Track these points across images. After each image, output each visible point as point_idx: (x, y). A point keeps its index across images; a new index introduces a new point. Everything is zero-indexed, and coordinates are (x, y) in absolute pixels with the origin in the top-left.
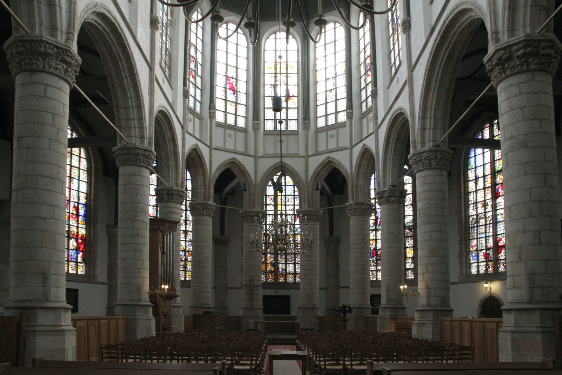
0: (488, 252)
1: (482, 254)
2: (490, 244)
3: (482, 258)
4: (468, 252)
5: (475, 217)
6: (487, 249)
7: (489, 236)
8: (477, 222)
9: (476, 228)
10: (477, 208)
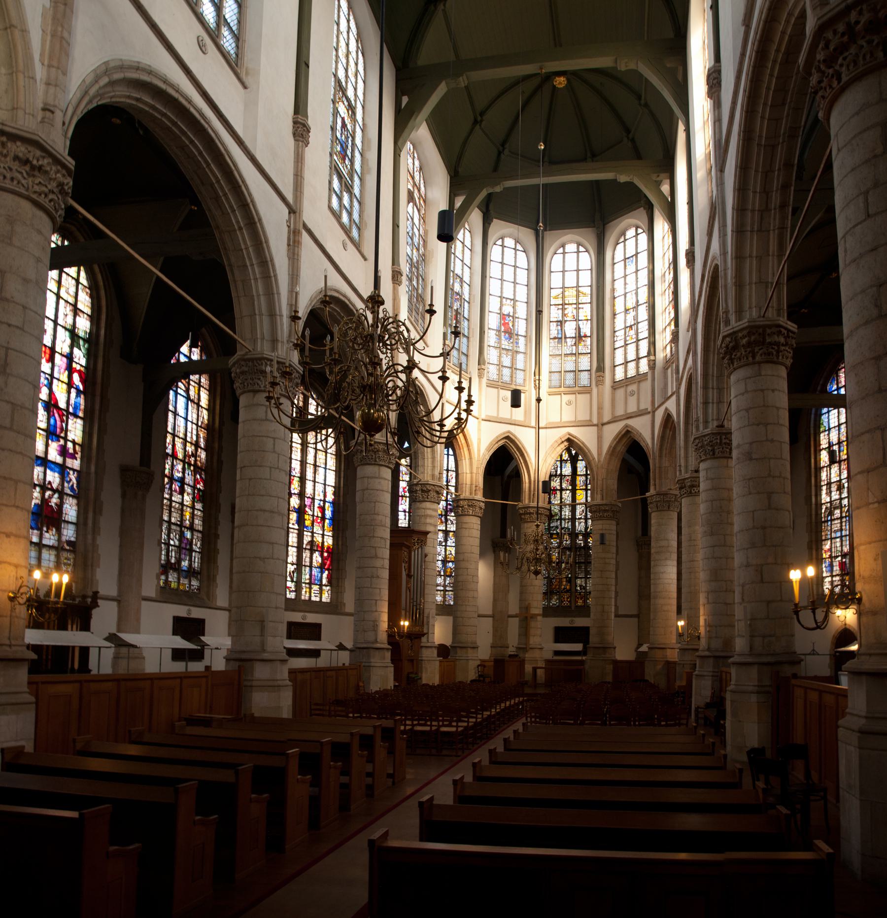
0: (844, 560)
5: (829, 505)
7: (846, 536)
8: (831, 513)
9: (829, 523)
10: (831, 492)
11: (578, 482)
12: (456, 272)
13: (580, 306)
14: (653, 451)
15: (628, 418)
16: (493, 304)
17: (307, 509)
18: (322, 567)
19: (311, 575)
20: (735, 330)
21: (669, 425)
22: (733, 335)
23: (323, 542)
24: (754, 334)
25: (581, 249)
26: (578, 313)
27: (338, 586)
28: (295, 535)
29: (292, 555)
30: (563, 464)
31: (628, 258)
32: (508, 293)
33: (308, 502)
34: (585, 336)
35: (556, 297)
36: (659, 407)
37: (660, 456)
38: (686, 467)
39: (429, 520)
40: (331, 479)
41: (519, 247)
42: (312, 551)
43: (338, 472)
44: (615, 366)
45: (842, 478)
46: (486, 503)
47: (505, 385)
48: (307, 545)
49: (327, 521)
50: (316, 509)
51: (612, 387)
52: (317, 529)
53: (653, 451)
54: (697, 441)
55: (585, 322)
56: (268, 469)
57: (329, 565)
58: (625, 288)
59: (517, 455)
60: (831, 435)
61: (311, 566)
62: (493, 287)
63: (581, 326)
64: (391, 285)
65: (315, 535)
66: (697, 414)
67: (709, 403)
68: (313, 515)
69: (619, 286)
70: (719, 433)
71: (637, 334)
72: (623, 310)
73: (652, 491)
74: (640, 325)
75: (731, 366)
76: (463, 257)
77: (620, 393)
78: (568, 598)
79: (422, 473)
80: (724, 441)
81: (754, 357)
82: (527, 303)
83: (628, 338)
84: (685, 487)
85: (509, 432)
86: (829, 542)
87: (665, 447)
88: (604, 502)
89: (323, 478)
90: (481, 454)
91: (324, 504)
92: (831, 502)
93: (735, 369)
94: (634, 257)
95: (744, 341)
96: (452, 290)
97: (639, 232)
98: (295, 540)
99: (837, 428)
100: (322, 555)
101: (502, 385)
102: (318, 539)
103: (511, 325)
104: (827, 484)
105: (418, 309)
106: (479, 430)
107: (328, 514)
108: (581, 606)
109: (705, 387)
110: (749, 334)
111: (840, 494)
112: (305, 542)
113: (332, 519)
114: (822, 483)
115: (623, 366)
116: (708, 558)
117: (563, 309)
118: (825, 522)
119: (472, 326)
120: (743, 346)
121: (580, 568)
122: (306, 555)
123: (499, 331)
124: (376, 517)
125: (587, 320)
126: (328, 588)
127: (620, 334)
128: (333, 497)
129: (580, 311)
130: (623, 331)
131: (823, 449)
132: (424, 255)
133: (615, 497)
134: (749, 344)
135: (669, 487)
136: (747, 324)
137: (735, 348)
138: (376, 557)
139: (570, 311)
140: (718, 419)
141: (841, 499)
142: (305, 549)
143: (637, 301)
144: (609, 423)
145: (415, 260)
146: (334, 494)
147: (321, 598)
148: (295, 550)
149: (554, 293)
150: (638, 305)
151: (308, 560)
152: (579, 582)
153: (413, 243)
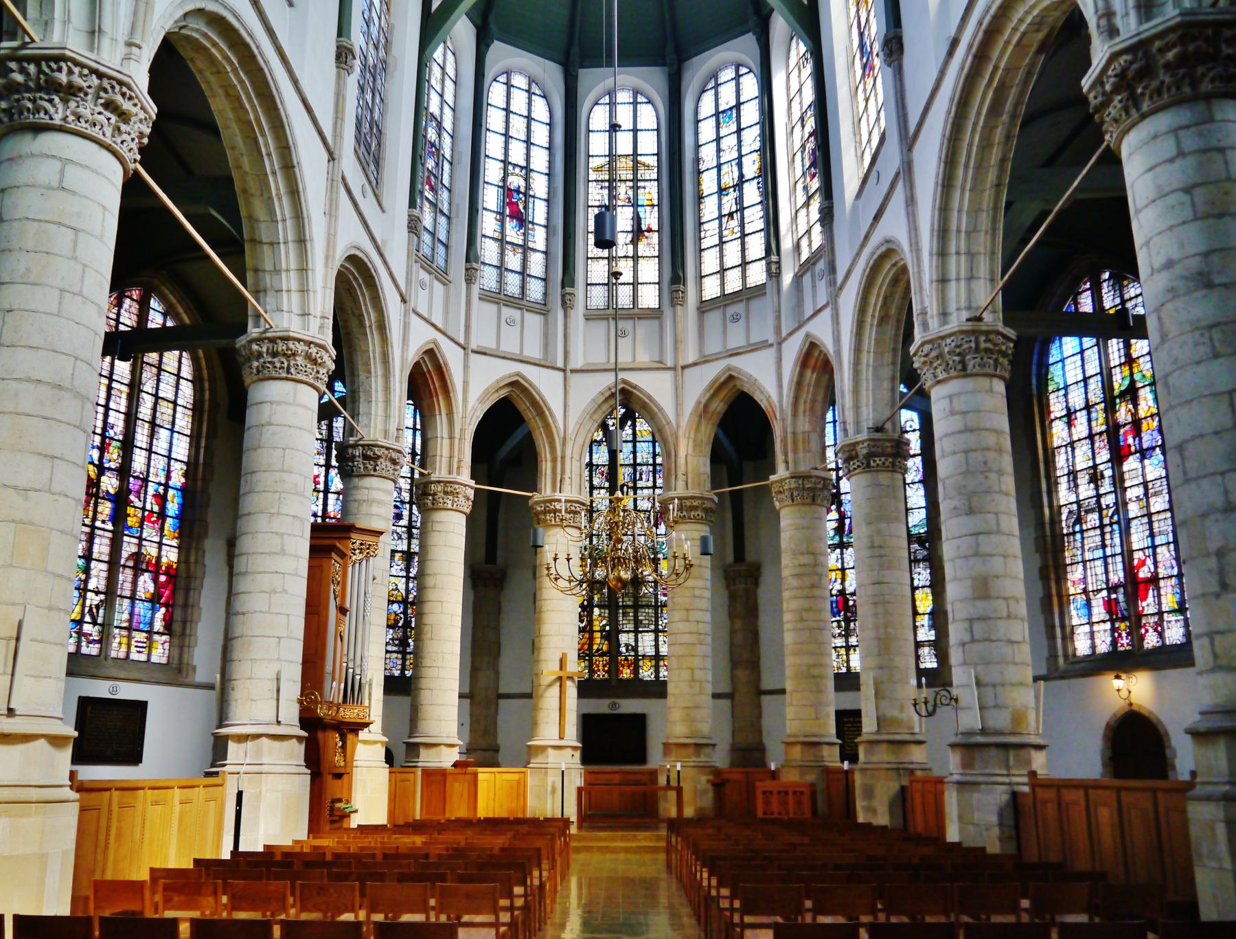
0: (1114, 596)
1: (1101, 601)
2: (1118, 575)
3: (1099, 612)
4: (1064, 600)
5: (1075, 507)
6: (1112, 589)
7: (1113, 556)
9: (1078, 536)
10: (1076, 486)
11: (620, 477)
12: (431, 110)
13: (640, 184)
14: (781, 406)
15: (731, 355)
16: (492, 172)
17: (132, 497)
18: (154, 600)
19: (131, 614)
20: (1143, 36)
21: (812, 362)
22: (1139, 48)
23: (159, 558)
24: (1194, 39)
25: (640, 99)
26: (636, 195)
27: (183, 635)
28: (107, 541)
29: (98, 576)
30: (594, 448)
31: (724, 112)
32: (517, 154)
33: (133, 484)
34: (649, 230)
35: (597, 170)
36: (790, 334)
37: (795, 415)
38: (857, 423)
39: (375, 509)
40: (182, 449)
41: (535, 89)
42: (137, 571)
43: (194, 438)
44: (702, 277)
45: (1098, 461)
46: (476, 490)
47: (511, 300)
48: (127, 559)
49: (169, 521)
50: (149, 498)
51: (698, 309)
52: (149, 532)
53: (781, 406)
54: (927, 348)
55: (648, 209)
56: (56, 293)
57: (169, 598)
58: (719, 157)
59: (529, 414)
60: (1069, 397)
61: (133, 598)
62: (493, 145)
63: (642, 215)
64: (334, 70)
65: (144, 543)
66: (922, 302)
67: (949, 280)
68: (144, 509)
69: (708, 153)
70: (973, 332)
71: (742, 225)
72: (715, 189)
73: (781, 472)
74: (746, 212)
75: (1133, 111)
76: (443, 89)
77: (714, 318)
78: (604, 666)
79: (366, 426)
80: (983, 345)
81: (1194, 84)
82: (548, 175)
83: (725, 233)
84: (857, 456)
85: (518, 374)
86: (1080, 567)
87: (802, 401)
88: (690, 493)
89: (166, 446)
90: (470, 407)
91: (166, 491)
92: (1078, 502)
93: (1143, 117)
94: (734, 111)
95: (1170, 55)
96: (425, 137)
97: (741, 73)
98: (106, 550)
99: (1082, 384)
100: (155, 580)
101: (507, 299)
102: (151, 550)
103: (521, 207)
104: (1068, 474)
105: (370, 146)
106: (466, 367)
107: (173, 508)
108: (628, 680)
109: (942, 253)
110: (1182, 40)
111: (1097, 488)
112: (125, 554)
113: (180, 517)
114: (1059, 473)
115: (718, 276)
116: (966, 557)
117: (612, 189)
118: (1068, 535)
119: (456, 200)
120: (1167, 66)
121: (625, 614)
122: (125, 577)
123: (502, 214)
124: (285, 476)
125: (653, 206)
126: (165, 638)
127: (711, 229)
128: (183, 480)
129: (641, 191)
130: (717, 221)
131: (1056, 418)
132: (385, 62)
133: (708, 485)
134: (1182, 60)
135: (813, 466)
136: (1178, 19)
137: (1146, 72)
138: (283, 552)
139: (623, 190)
140: (969, 308)
141: (1099, 496)
142: (125, 566)
143: (741, 176)
144: (695, 364)
145: (371, 61)
146: (186, 475)
147: (149, 655)
148: (104, 567)
149: (594, 163)
150: (742, 180)
151: (128, 586)
152: (624, 638)
153: (369, 34)
